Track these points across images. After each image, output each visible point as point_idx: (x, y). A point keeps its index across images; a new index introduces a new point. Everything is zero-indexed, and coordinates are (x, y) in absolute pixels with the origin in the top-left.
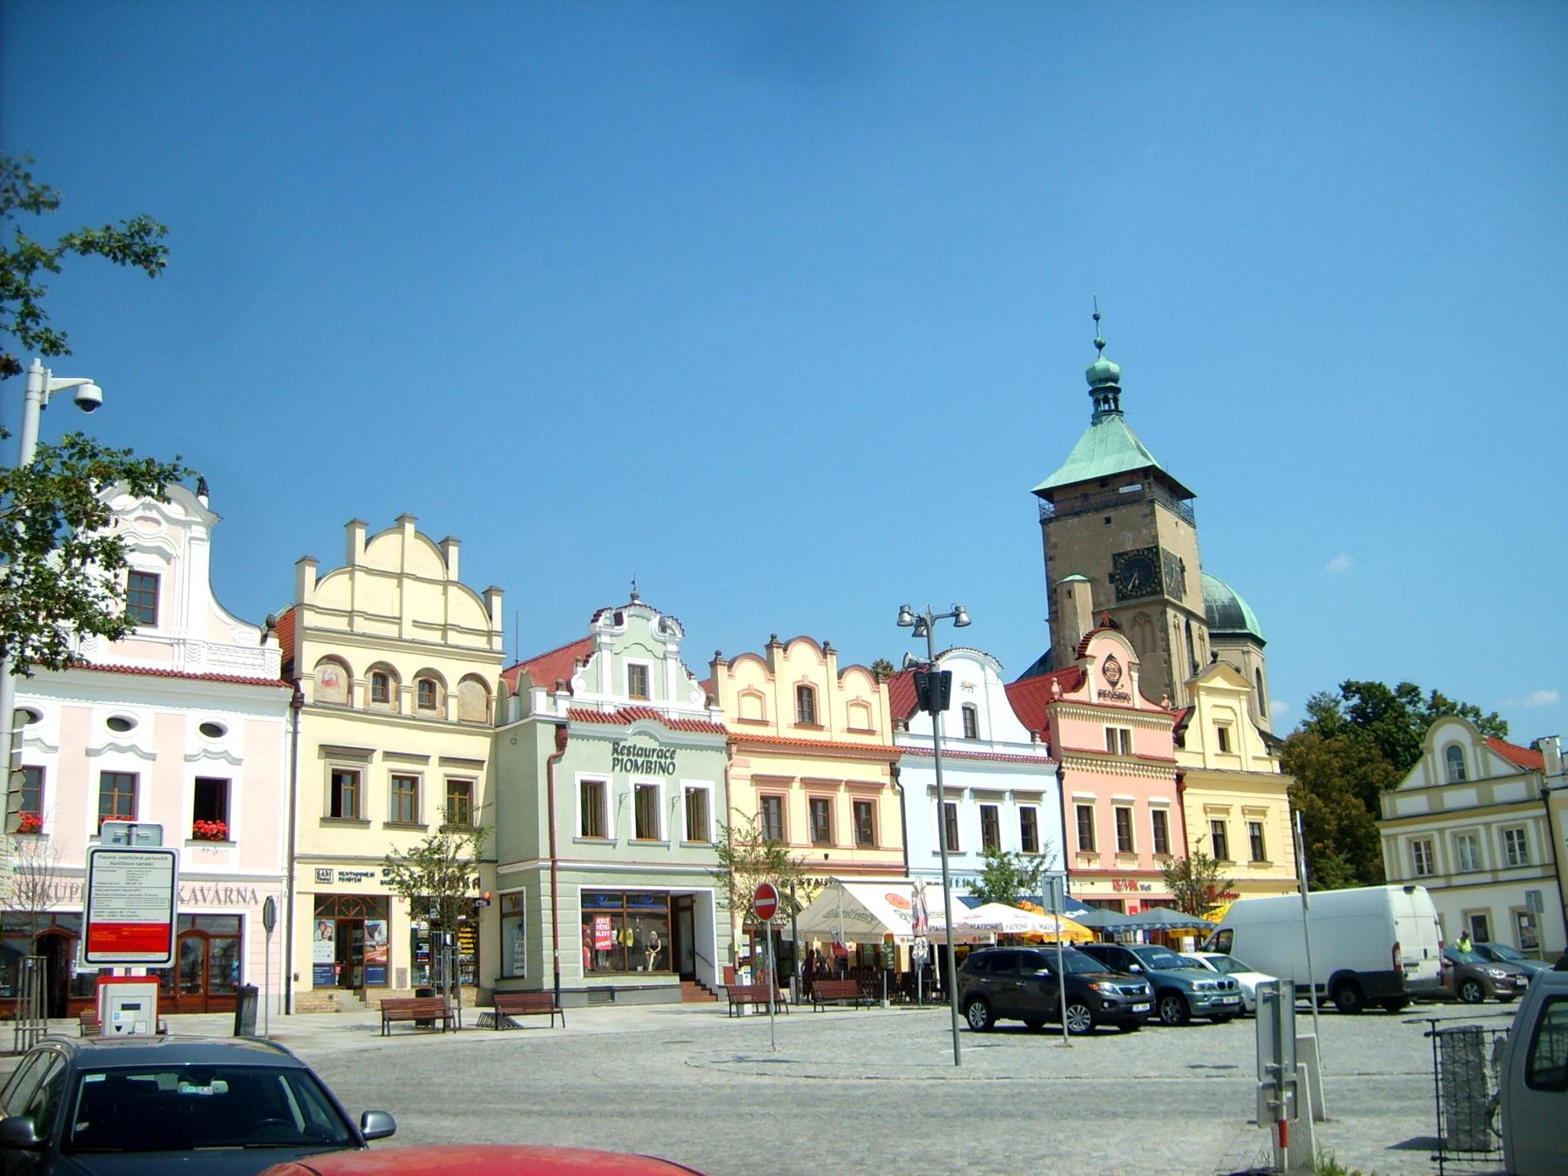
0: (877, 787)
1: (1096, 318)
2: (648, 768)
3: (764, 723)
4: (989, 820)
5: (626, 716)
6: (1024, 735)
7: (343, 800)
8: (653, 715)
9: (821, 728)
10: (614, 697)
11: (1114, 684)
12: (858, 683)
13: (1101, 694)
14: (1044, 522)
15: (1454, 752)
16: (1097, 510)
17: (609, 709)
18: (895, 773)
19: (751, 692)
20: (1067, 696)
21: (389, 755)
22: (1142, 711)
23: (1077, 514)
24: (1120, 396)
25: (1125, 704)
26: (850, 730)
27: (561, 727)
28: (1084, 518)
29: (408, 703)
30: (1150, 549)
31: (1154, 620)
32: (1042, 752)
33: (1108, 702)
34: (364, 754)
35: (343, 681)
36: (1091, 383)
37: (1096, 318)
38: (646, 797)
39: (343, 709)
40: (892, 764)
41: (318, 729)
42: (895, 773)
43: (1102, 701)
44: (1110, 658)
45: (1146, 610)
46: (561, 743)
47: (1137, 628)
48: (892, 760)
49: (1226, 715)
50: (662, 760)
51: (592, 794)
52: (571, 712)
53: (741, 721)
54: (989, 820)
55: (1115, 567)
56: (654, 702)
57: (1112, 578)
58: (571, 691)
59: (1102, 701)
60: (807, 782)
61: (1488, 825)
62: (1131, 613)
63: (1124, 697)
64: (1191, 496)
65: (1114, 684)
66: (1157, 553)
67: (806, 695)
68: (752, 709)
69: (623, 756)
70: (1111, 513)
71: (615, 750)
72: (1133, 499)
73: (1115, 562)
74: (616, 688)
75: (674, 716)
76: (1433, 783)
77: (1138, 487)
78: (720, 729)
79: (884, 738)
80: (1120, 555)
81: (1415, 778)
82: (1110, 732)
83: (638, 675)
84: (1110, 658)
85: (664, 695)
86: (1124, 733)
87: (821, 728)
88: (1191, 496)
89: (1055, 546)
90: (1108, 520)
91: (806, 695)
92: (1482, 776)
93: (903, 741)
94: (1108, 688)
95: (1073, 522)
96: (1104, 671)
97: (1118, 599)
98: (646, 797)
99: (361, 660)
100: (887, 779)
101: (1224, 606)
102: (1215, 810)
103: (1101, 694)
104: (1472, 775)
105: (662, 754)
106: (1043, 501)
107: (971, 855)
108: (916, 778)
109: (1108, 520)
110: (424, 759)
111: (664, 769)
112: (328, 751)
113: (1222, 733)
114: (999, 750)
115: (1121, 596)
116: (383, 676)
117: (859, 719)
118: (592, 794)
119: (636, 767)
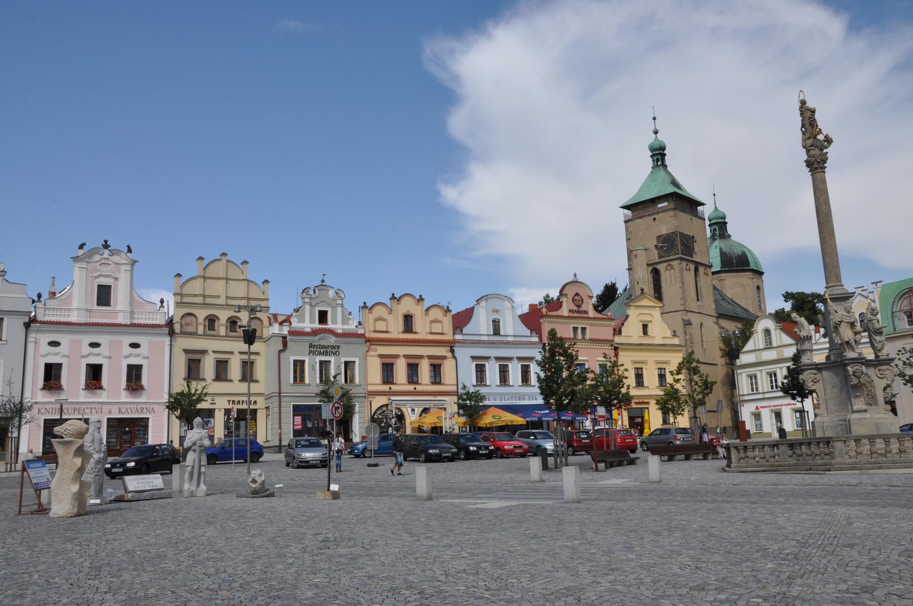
0: (444, 358)
1: (654, 119)
2: (326, 354)
3: (387, 332)
4: (504, 371)
5: (315, 333)
6: (528, 332)
7: (193, 369)
8: (332, 332)
9: (416, 333)
10: (309, 324)
11: (579, 306)
12: (436, 313)
13: (571, 311)
14: (625, 222)
15: (767, 332)
16: (650, 215)
17: (308, 330)
18: (452, 351)
19: (380, 319)
20: (550, 313)
21: (214, 352)
22: (594, 319)
23: (640, 217)
24: (666, 157)
25: (586, 315)
26: (431, 333)
27: (284, 338)
28: (644, 219)
29: (222, 331)
31: (675, 267)
32: (536, 339)
33: (576, 315)
34: (204, 352)
35: (194, 324)
36: (652, 151)
37: (654, 119)
38: (324, 365)
39: (194, 334)
40: (452, 347)
41: (184, 343)
42: (452, 351)
43: (571, 314)
44: (577, 294)
46: (285, 344)
48: (451, 345)
49: (645, 318)
50: (334, 350)
51: (299, 366)
52: (289, 332)
53: (375, 331)
54: (504, 371)
56: (330, 325)
57: (656, 246)
58: (291, 323)
59: (571, 314)
60: (430, 357)
62: (665, 265)
63: (586, 312)
64: (703, 204)
65: (579, 306)
67: (408, 319)
68: (381, 326)
69: (314, 349)
70: (656, 216)
71: (310, 347)
72: (664, 210)
74: (312, 321)
75: (340, 331)
77: (666, 204)
78: (363, 336)
79: (449, 337)
80: (660, 236)
81: (749, 346)
82: (575, 329)
83: (323, 317)
84: (577, 294)
85: (334, 322)
86: (584, 329)
87: (416, 333)
88: (703, 204)
89: (631, 233)
90: (654, 219)
91: (408, 319)
93: (458, 337)
94: (576, 308)
95: (639, 221)
96: (573, 300)
98: (324, 365)
99: (202, 314)
100: (449, 355)
101: (739, 256)
102: (658, 363)
103: (571, 311)
104: (774, 344)
105: (333, 347)
106: (626, 211)
107: (494, 386)
108: (463, 354)
109: (654, 219)
110: (232, 353)
111: (335, 354)
112: (186, 351)
113: (645, 327)
114: (511, 339)
115: (660, 256)
116: (211, 321)
117: (437, 328)
118: (299, 366)
119: (320, 353)
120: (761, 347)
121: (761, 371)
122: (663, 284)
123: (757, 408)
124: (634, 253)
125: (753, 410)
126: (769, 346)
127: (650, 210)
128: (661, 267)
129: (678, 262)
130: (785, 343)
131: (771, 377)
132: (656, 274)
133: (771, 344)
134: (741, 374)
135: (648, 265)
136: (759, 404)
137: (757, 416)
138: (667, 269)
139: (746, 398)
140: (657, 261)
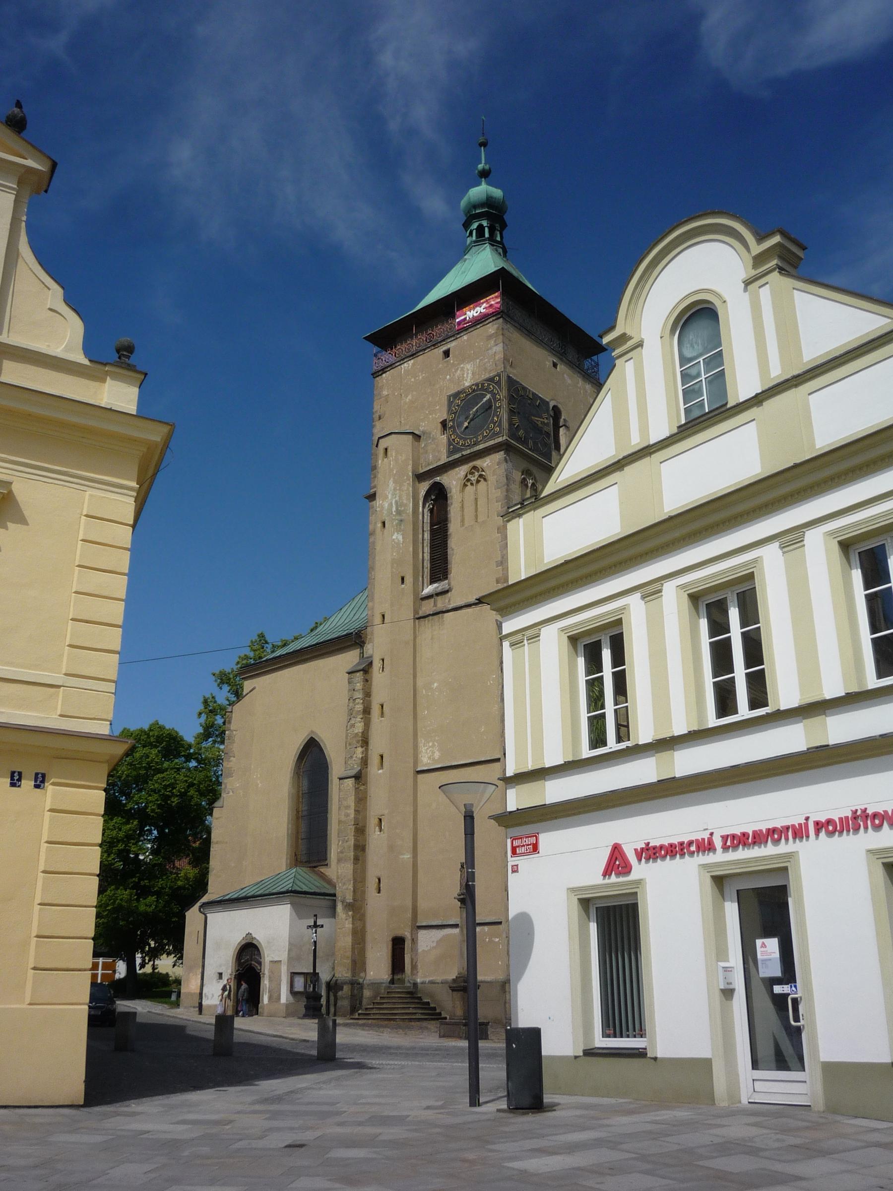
16: (435, 345)
23: (413, 356)
30: (491, 380)
31: (488, 473)
45: (478, 463)
47: (469, 487)
55: (450, 411)
57: (444, 424)
61: (790, 539)
62: (462, 471)
66: (498, 383)
70: (452, 345)
73: (450, 403)
76: (636, 442)
80: (456, 395)
90: (447, 354)
92: (777, 373)
97: (450, 453)
104: (744, 383)
109: (447, 354)
120: (660, 430)
121: (650, 591)
122: (454, 527)
123: (617, 862)
124: (383, 443)
125: (591, 874)
126: (707, 412)
127: (439, 330)
128: (452, 480)
129: (500, 456)
130: (814, 350)
131: (719, 626)
132: (438, 497)
133: (719, 380)
134: (532, 633)
135: (420, 477)
136: (634, 830)
137: (617, 924)
138: (467, 482)
139: (557, 791)
140: (444, 459)
